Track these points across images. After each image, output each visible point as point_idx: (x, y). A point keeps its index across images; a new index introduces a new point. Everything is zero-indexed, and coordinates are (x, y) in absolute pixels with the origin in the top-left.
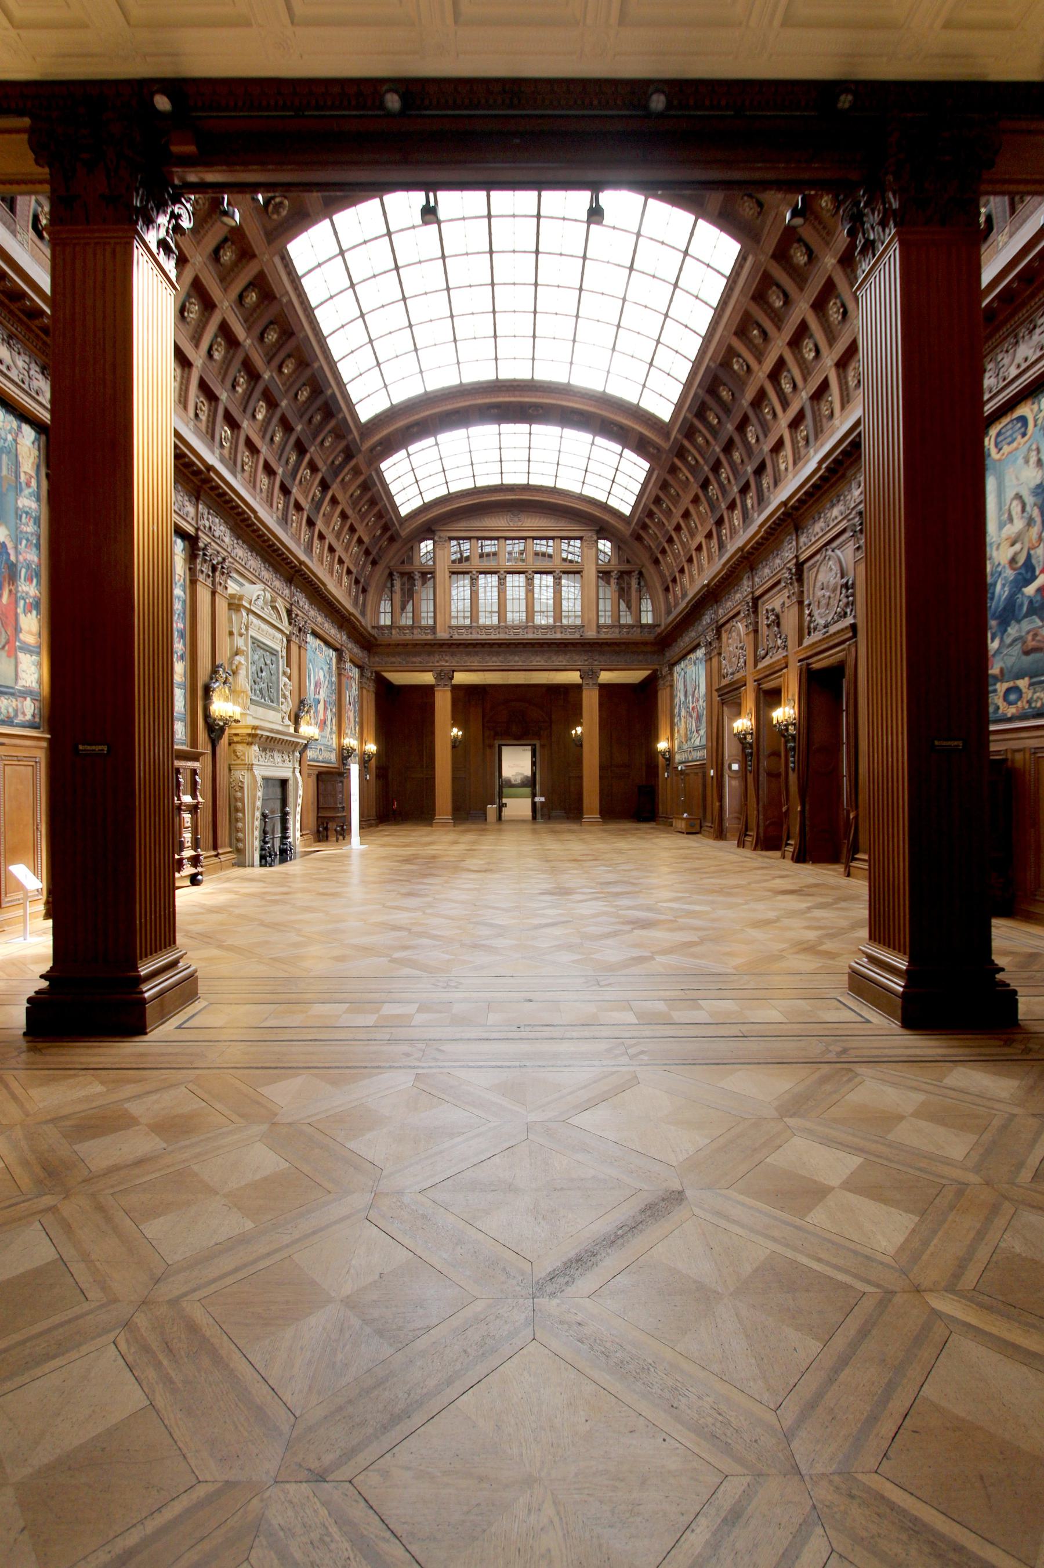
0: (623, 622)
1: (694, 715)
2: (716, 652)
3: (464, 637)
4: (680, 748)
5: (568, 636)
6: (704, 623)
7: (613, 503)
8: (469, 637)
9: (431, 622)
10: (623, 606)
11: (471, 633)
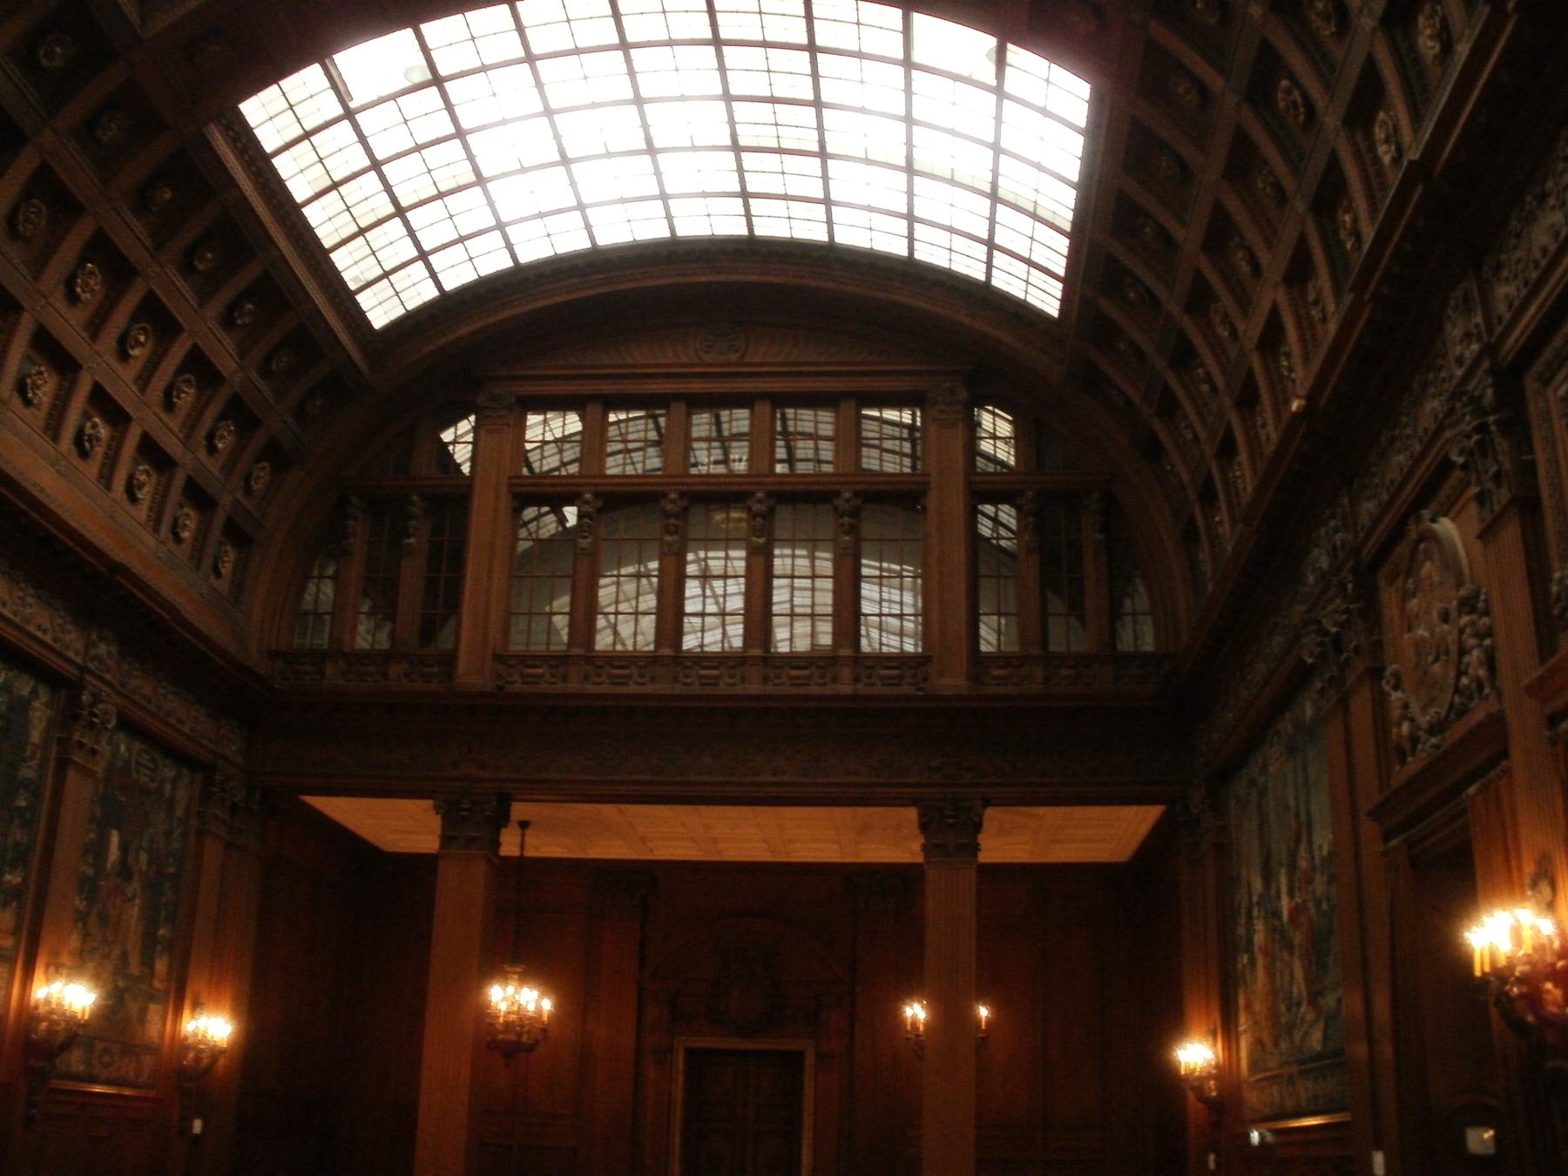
0: (1056, 646)
1: (1298, 937)
2: (1360, 665)
3: (543, 687)
4: (1254, 1065)
5: (878, 689)
6: (1311, 579)
7: (1009, 280)
8: (560, 687)
9: (449, 646)
10: (1056, 604)
11: (565, 679)
